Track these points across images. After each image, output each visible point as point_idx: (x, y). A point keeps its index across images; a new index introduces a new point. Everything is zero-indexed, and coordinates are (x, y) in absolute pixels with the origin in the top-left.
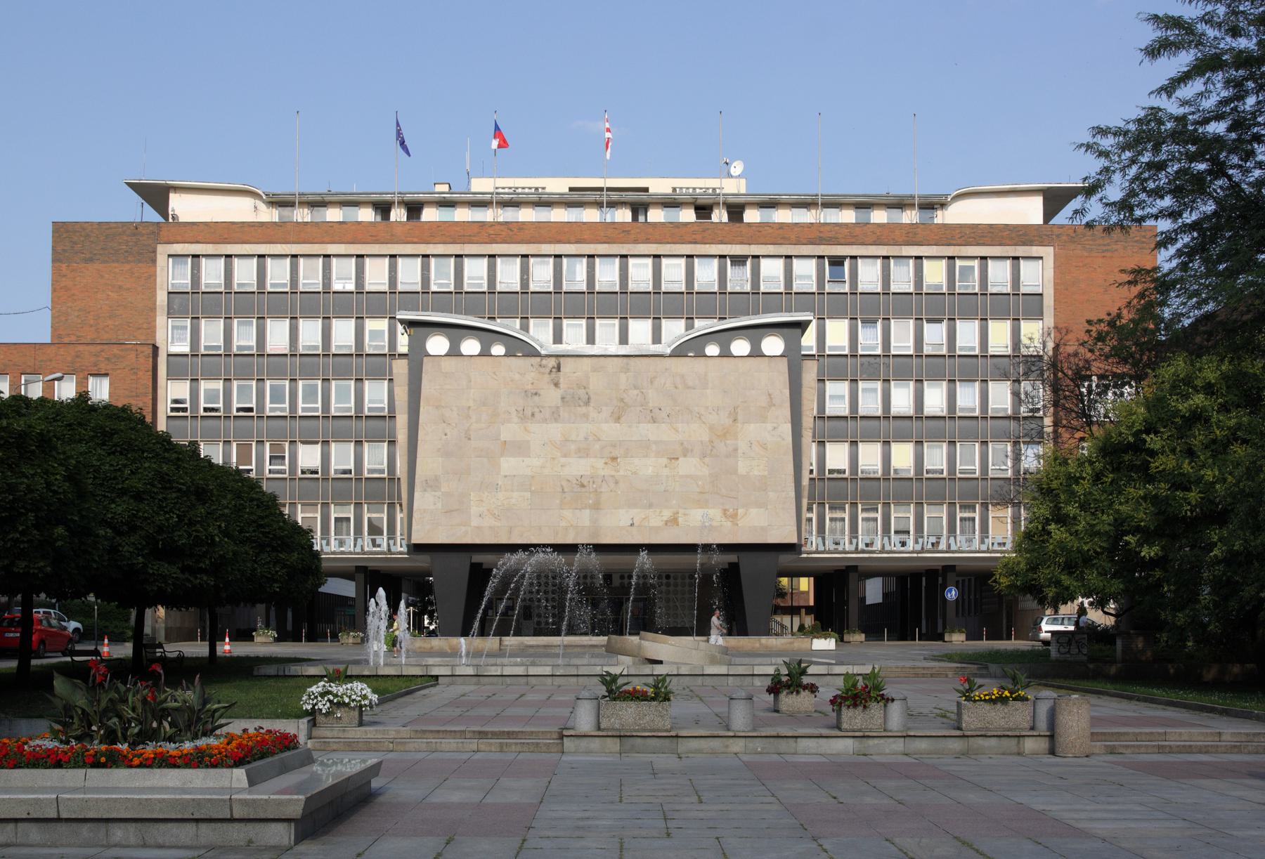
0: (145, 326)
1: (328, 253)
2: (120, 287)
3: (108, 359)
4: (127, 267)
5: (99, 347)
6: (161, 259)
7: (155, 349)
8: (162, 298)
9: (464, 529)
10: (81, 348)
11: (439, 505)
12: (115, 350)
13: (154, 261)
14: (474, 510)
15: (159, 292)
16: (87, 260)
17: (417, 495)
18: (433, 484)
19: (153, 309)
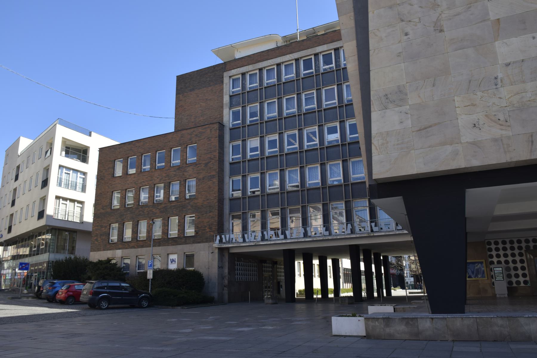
0: (219, 116)
1: (317, 51)
2: (207, 99)
3: (196, 135)
4: (210, 88)
5: (192, 130)
6: (226, 80)
7: (222, 126)
8: (226, 99)
9: (449, 148)
10: (184, 132)
11: (409, 123)
12: (200, 129)
13: (223, 82)
14: (463, 120)
15: (224, 96)
16: (191, 90)
17: (375, 116)
18: (397, 98)
19: (222, 107)
